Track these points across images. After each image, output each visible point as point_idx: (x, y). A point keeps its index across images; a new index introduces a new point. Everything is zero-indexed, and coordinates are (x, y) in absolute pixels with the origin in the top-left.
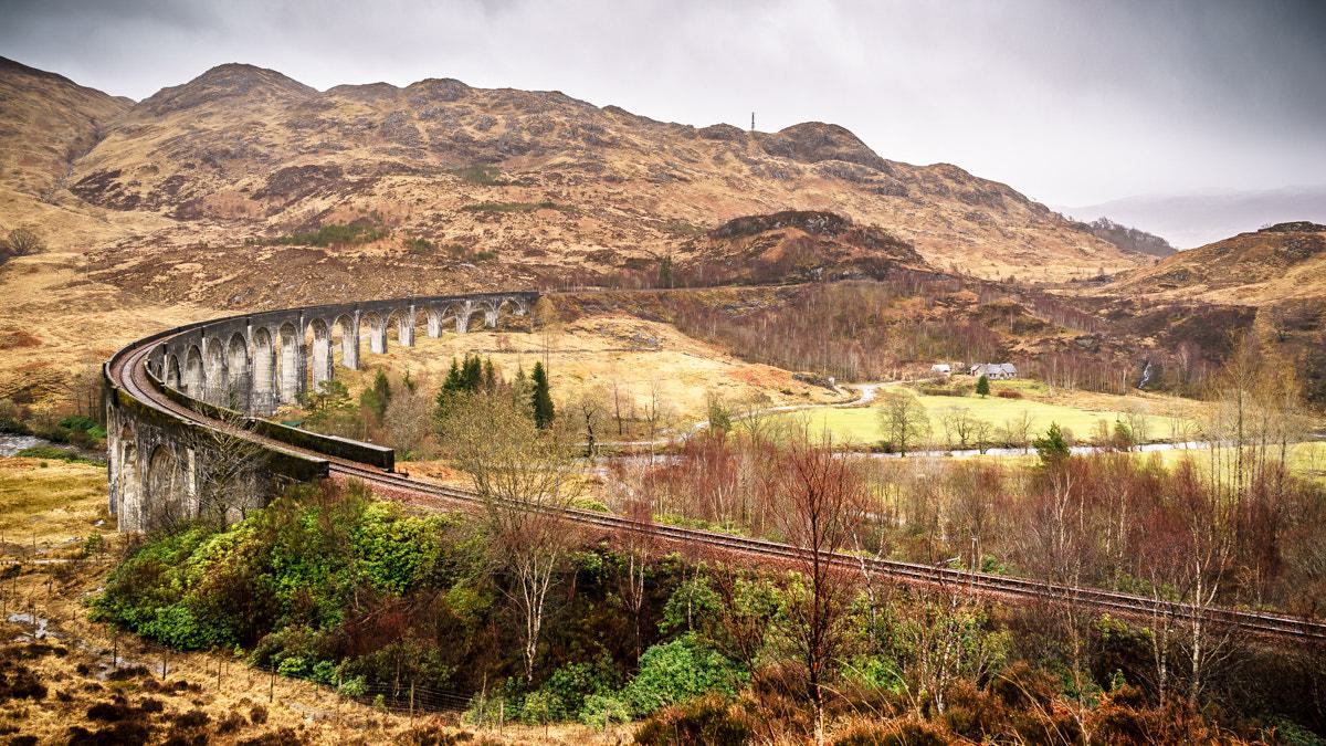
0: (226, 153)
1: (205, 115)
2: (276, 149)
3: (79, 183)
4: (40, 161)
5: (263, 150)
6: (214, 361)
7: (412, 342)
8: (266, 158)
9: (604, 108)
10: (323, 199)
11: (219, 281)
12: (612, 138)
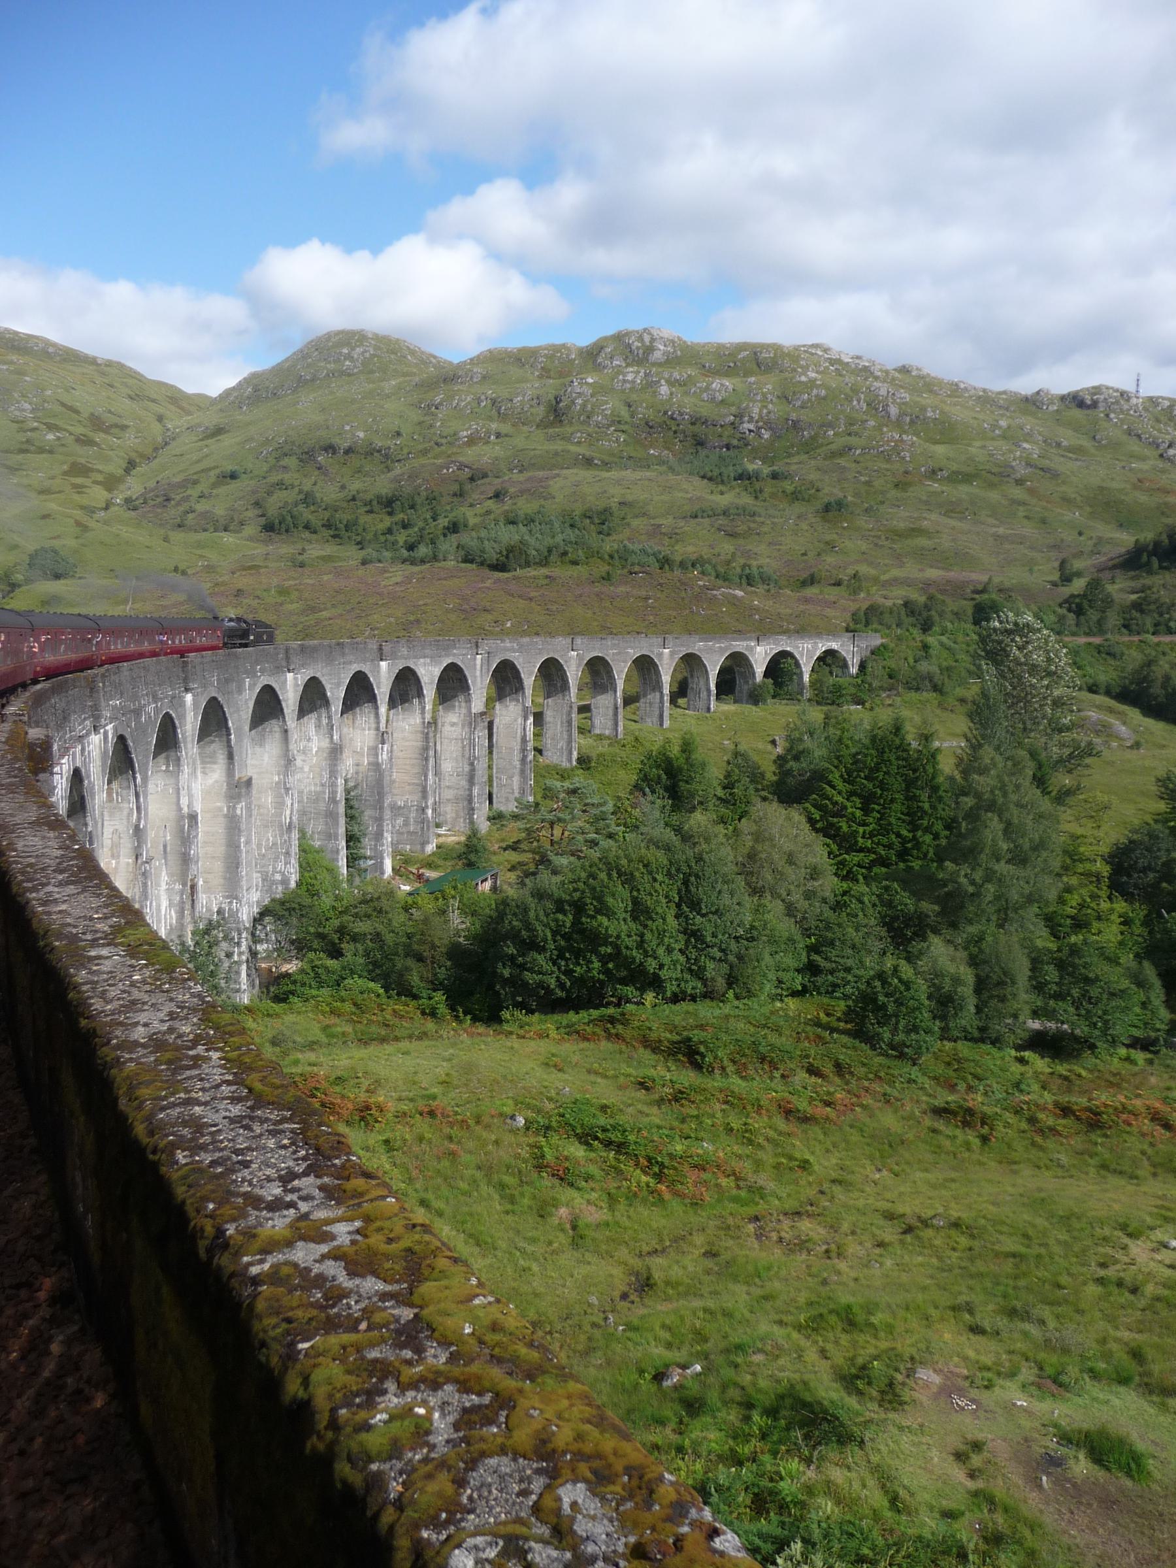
0: (330, 449)
11: (325, 614)
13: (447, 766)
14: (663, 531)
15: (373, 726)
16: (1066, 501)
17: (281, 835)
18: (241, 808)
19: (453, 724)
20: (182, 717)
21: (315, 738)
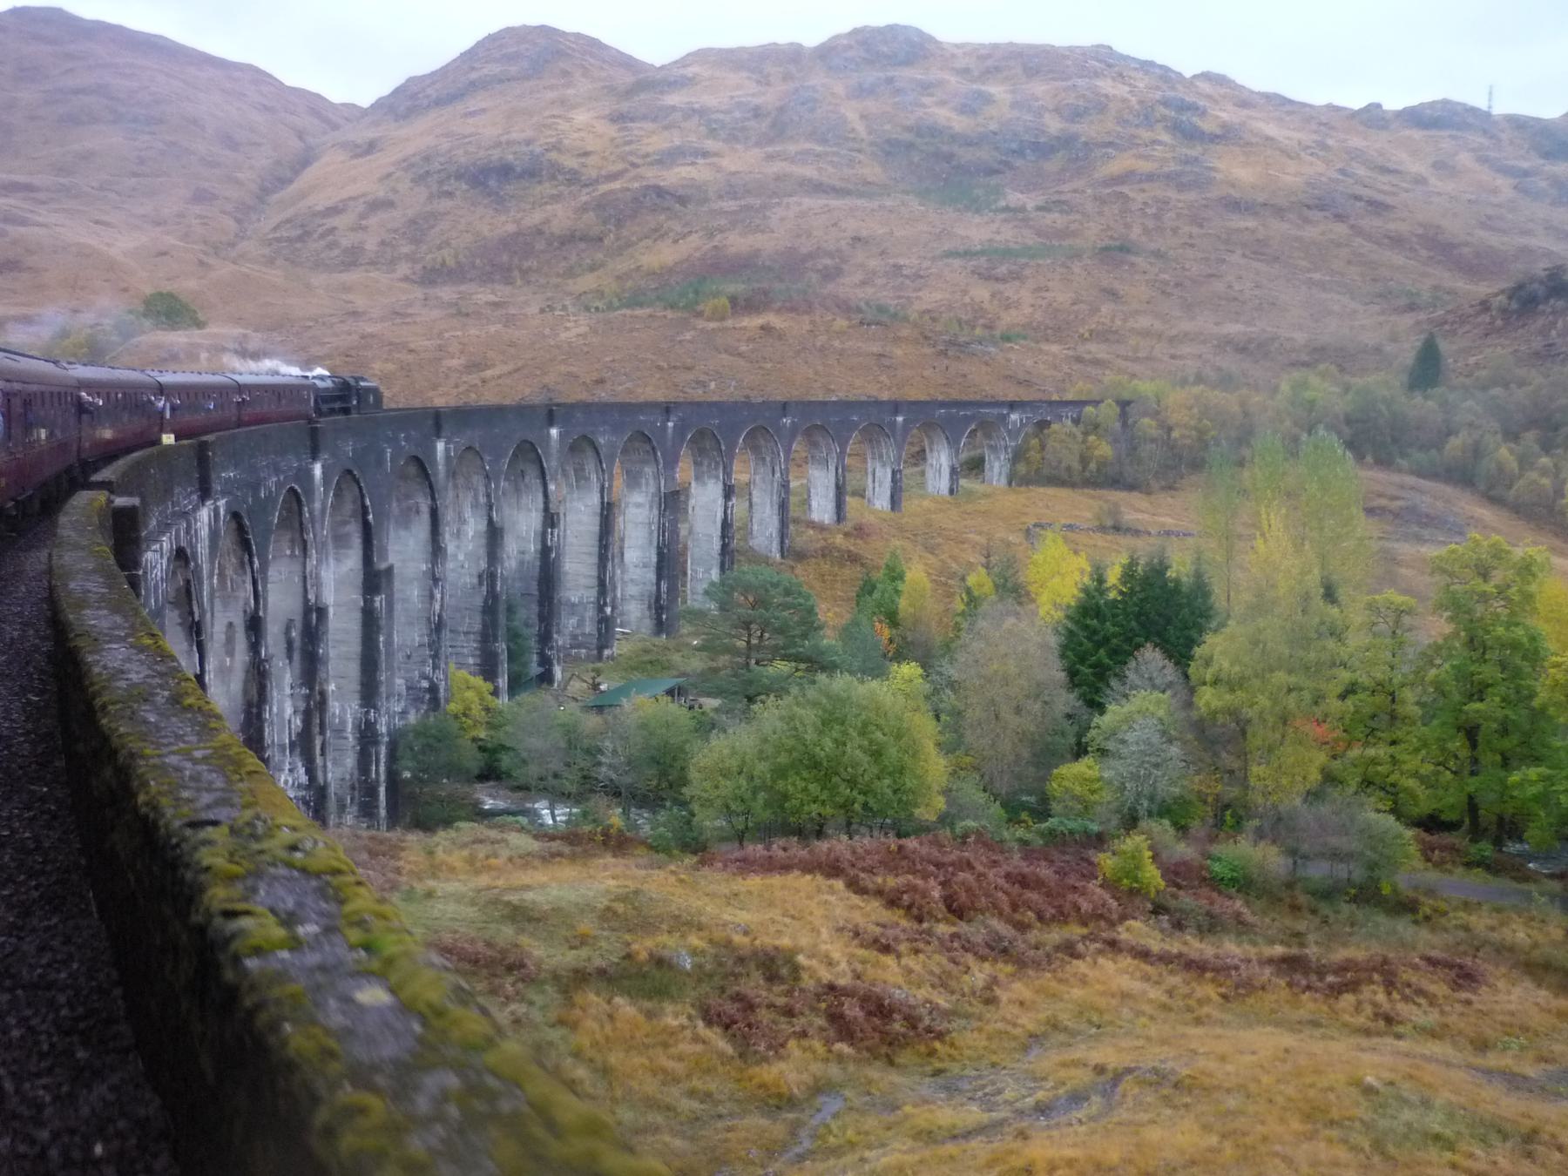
0: (505, 171)
1: (472, 114)
2: (591, 160)
3: (275, 229)
4: (214, 197)
5: (570, 162)
6: (468, 513)
7: (895, 502)
8: (573, 178)
9: (1195, 77)
10: (676, 241)
12: (1224, 126)
13: (632, 556)
14: (905, 272)
15: (541, 506)
16: (1397, 241)
17: (430, 635)
18: (379, 601)
19: (638, 505)
20: (310, 491)
21: (472, 521)
